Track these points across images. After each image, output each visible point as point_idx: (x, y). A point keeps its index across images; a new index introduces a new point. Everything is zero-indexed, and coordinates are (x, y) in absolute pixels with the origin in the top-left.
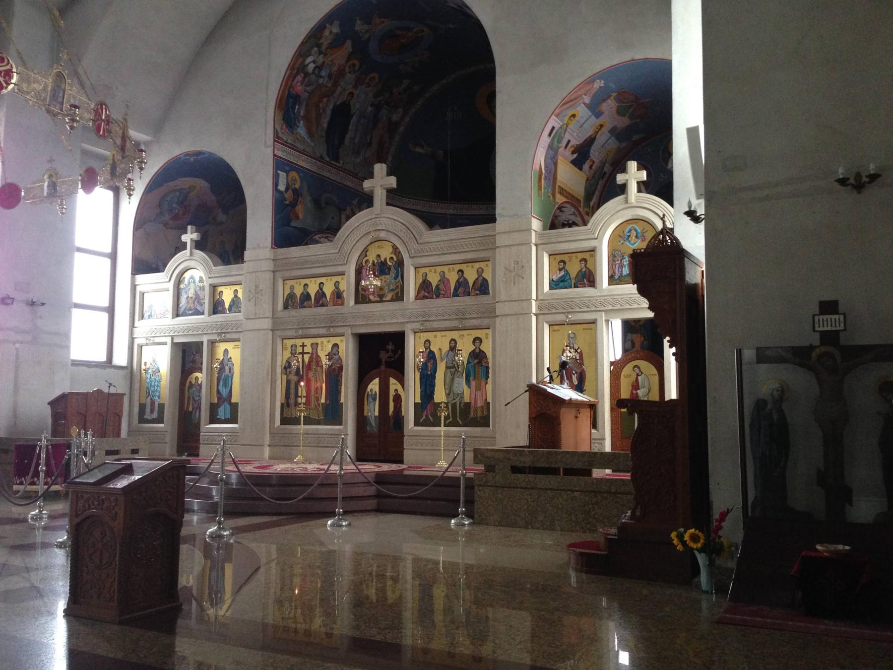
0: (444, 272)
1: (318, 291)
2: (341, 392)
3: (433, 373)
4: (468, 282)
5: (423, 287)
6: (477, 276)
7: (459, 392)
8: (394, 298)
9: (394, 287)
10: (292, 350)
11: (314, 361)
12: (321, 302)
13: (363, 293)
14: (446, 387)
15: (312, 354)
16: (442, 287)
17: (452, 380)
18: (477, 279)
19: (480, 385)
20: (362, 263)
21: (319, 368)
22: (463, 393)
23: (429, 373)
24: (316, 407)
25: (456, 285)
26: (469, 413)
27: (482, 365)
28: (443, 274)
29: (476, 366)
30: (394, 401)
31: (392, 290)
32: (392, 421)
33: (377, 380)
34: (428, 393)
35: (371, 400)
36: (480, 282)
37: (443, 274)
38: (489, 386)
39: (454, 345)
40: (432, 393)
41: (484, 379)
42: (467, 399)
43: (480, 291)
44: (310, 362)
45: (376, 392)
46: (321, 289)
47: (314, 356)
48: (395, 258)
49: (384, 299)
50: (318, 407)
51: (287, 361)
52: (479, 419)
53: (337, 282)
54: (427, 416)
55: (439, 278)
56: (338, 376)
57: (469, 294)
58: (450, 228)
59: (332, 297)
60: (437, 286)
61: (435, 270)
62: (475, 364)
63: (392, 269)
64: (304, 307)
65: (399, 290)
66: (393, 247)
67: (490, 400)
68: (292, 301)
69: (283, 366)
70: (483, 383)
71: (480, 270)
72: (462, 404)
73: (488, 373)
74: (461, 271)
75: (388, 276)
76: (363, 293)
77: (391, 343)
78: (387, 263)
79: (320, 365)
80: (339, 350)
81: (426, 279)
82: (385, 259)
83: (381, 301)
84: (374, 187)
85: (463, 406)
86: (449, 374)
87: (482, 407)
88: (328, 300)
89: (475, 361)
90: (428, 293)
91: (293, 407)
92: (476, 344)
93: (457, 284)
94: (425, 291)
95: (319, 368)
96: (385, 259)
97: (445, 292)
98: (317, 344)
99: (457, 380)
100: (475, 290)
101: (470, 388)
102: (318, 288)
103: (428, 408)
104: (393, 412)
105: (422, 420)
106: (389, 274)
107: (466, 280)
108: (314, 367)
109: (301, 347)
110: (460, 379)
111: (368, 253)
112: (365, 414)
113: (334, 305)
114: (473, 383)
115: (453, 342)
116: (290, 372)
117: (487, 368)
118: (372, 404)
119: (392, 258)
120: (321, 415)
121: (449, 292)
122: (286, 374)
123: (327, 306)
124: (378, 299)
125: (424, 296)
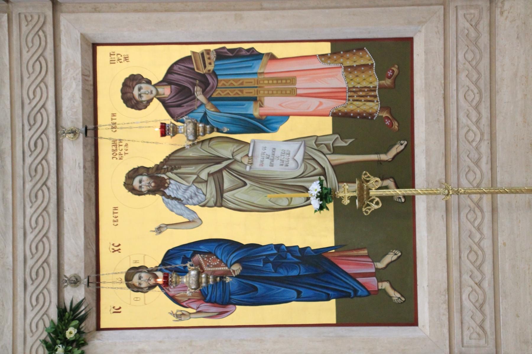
3: (233, 257)
7: (299, 157)
19: (279, 80)
23: (237, 268)
26: (367, 117)
27: (214, 74)
29: (215, 95)
41: (258, 67)
52: (388, 82)
54: (380, 275)
62: (210, 99)
67: (326, 48)
70: (272, 68)
72: (341, 143)
73: (236, 54)
85: (342, 139)
86: (241, 194)
101: (285, 117)
103: (351, 269)
105: (395, 295)
117: (221, 55)
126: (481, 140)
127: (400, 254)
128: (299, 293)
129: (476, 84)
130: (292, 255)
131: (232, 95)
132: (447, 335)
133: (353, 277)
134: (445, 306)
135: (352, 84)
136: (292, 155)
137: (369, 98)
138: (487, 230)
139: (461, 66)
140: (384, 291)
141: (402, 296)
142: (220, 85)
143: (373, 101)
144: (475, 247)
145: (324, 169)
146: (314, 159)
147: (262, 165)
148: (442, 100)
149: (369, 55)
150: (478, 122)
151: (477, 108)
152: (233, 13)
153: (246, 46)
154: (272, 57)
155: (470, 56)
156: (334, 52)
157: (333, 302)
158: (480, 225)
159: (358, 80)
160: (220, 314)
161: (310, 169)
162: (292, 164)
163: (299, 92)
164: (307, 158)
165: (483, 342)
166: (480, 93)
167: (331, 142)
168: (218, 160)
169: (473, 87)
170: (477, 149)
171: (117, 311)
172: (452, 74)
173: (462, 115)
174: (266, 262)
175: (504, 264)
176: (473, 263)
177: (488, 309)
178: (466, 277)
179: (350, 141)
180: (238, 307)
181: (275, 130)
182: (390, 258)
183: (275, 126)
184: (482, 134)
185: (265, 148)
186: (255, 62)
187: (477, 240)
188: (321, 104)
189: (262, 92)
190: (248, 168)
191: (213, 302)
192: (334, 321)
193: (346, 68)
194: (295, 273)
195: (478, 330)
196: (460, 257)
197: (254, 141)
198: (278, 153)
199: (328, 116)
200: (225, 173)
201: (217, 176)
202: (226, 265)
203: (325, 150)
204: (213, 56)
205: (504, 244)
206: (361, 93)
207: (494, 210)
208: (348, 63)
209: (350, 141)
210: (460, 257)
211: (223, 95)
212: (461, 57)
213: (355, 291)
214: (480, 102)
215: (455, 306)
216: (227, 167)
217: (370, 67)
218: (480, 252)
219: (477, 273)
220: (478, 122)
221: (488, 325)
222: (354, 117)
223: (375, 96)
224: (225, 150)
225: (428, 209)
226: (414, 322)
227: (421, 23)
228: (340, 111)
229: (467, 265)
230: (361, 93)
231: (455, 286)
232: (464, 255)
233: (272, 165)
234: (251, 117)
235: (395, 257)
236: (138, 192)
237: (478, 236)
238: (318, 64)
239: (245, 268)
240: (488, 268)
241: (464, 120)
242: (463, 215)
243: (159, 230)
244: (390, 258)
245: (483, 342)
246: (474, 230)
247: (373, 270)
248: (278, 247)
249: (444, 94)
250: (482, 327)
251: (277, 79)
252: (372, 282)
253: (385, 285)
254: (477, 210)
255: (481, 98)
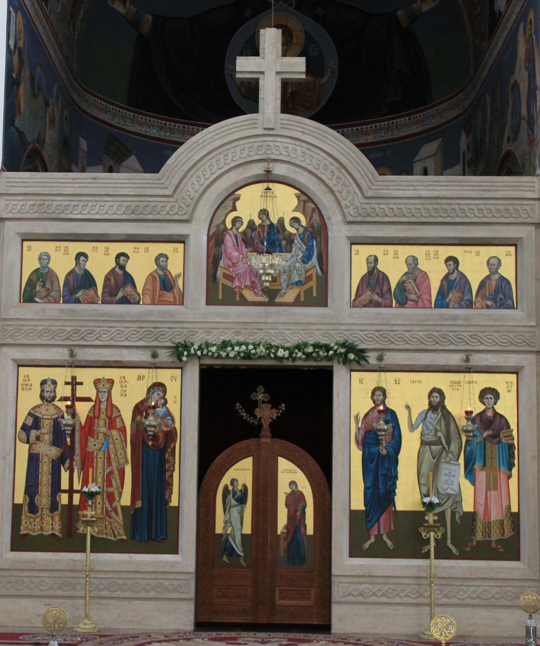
0: (415, 259)
1: (113, 270)
2: (172, 485)
3: (391, 451)
4: (467, 282)
5: (368, 286)
6: (488, 273)
7: (450, 491)
8: (302, 299)
9: (303, 279)
10: (42, 391)
11: (103, 416)
12: (120, 295)
13: (228, 283)
14: (423, 481)
15: (98, 401)
16: (410, 285)
17: (435, 469)
18: (488, 278)
19: (495, 480)
20: (224, 222)
21: (115, 433)
22: (460, 494)
23: (384, 452)
24: (108, 514)
25: (442, 286)
26: (473, 531)
27: (500, 442)
28: (412, 262)
29: (487, 442)
30: (287, 505)
31: (299, 283)
32: (283, 545)
33: (247, 463)
34: (382, 491)
35: (234, 502)
36: (494, 282)
37: (412, 262)
38: (513, 482)
39: (438, 399)
40: (391, 493)
41: (503, 469)
42: (468, 506)
43: (494, 300)
44: (90, 420)
45: (245, 487)
46: (122, 268)
47: (103, 406)
48: (304, 222)
49: (278, 300)
50: (113, 514)
51: (30, 414)
52: (494, 545)
53: (161, 255)
54: (379, 537)
55: (406, 270)
56: (163, 451)
57: (470, 305)
58: (506, 175)
59: (149, 286)
60: (401, 285)
61: (396, 253)
62: (485, 439)
63: (297, 241)
64: (78, 301)
65: (313, 283)
66: (298, 197)
67: (514, 509)
68: (43, 286)
69: (20, 425)
70: (503, 477)
71: (492, 261)
72: (457, 516)
73: (511, 456)
74: (453, 261)
75: (288, 255)
76: (228, 283)
77: (261, 388)
78: (284, 229)
79: (119, 425)
80: (167, 397)
81: (375, 267)
82: (281, 221)
83: (271, 303)
84: (263, 73)
85: (460, 517)
86: (428, 456)
87: (502, 522)
88: (140, 290)
89: (486, 434)
90: (382, 296)
91: (46, 512)
92: (486, 401)
93: (445, 283)
94: (373, 290)
95: (115, 433)
96: (281, 221)
97: (419, 297)
98: (111, 382)
99: (444, 468)
100: (484, 297)
101: (473, 483)
102: (114, 265)
103: (382, 519)
104: (286, 527)
105: (367, 545)
106: (290, 251)
107: (463, 276)
108: (104, 430)
109: (69, 387)
110: (453, 467)
111: (238, 204)
112: (219, 530)
113: (153, 303)
114: (481, 476)
115: (435, 394)
116: (38, 438)
117: (511, 447)
118: (235, 512)
119: (295, 220)
120: (121, 531)
121: (425, 297)
122: (28, 442)
123: (138, 303)
124: (265, 299)
125: (371, 301)
126: (459, 599)
127: (391, 548)
128: (369, 488)
129: (493, 597)
130: (391, 486)
131: (487, 452)
132: (344, 574)
133: (378, 520)
134: (362, 574)
135: (493, 524)
136: (451, 487)
137: (484, 534)
138: (406, 600)
139: (503, 588)
140: (369, 539)
141: (367, 549)
142: (493, 445)
143: (482, 536)
144: (396, 593)
145: (442, 505)
146: (448, 499)
147: (445, 469)
148: (483, 576)
149: (510, 535)
150: (470, 597)
151: (478, 597)
152: (536, 455)
153: (516, 462)
154: (509, 477)
155: (509, 594)
156: (513, 514)
157: (363, 508)
158: (409, 596)
159: (495, 527)
160: (357, 442)
161: (443, 497)
162: (445, 487)
163: (489, 492)
164: (449, 496)
165: (341, 594)
166: (487, 599)
167: (458, 510)
168: (448, 443)
169: (490, 595)
170: (454, 596)
171: (361, 382)
172: (499, 583)
173: (474, 588)
174: (388, 469)
175: (385, 610)
176: (386, 591)
177: (360, 599)
178: (378, 587)
179: (459, 522)
180: (361, 452)
181: (466, 477)
182: (389, 543)
183: (469, 478)
184: (463, 600)
185: (455, 471)
186: (507, 467)
187: (400, 594)
188: (481, 505)
189: (489, 470)
190: (443, 460)
191: (365, 438)
192: (352, 508)
193: (502, 521)
194: (381, 486)
195: (348, 592)
196: (390, 584)
197: (459, 464)
198: (452, 478)
199: (474, 509)
200: (440, 447)
201: (438, 442)
202: (386, 446)
203: (454, 507)
204: (510, 442)
205: (397, 610)
206: (487, 529)
207: (417, 605)
208: (505, 522)
209: (459, 522)
210: (390, 584)
211: (487, 447)
212: (509, 588)
213: (370, 522)
214: (482, 599)
215: (362, 580)
216: (444, 448)
217: (503, 534)
218: (392, 595)
219: (380, 593)
220: (470, 597)
221: (350, 598)
222: (473, 525)
223: (485, 537)
224: (454, 447)
225: (419, 566)
226: (352, 555)
227: (529, 566)
228: (477, 516)
229: (386, 588)
230: (487, 529)
231: (373, 580)
232: (391, 586)
233: (445, 474)
234: (474, 464)
235: (389, 546)
236: (430, 395)
237: (402, 594)
238: (505, 505)
239: (384, 457)
240: (383, 599)
241: (471, 589)
242: (415, 587)
243: (408, 407)
244: (389, 543)
245: (341, 594)
246: (406, 592)
247: (382, 532)
248: (396, 477)
249: (487, 578)
250: (349, 594)
251: (496, 480)
252: (375, 532)
253: (373, 540)
254: (417, 595)
255: (484, 600)
